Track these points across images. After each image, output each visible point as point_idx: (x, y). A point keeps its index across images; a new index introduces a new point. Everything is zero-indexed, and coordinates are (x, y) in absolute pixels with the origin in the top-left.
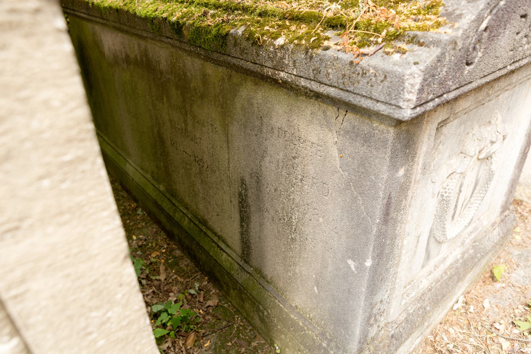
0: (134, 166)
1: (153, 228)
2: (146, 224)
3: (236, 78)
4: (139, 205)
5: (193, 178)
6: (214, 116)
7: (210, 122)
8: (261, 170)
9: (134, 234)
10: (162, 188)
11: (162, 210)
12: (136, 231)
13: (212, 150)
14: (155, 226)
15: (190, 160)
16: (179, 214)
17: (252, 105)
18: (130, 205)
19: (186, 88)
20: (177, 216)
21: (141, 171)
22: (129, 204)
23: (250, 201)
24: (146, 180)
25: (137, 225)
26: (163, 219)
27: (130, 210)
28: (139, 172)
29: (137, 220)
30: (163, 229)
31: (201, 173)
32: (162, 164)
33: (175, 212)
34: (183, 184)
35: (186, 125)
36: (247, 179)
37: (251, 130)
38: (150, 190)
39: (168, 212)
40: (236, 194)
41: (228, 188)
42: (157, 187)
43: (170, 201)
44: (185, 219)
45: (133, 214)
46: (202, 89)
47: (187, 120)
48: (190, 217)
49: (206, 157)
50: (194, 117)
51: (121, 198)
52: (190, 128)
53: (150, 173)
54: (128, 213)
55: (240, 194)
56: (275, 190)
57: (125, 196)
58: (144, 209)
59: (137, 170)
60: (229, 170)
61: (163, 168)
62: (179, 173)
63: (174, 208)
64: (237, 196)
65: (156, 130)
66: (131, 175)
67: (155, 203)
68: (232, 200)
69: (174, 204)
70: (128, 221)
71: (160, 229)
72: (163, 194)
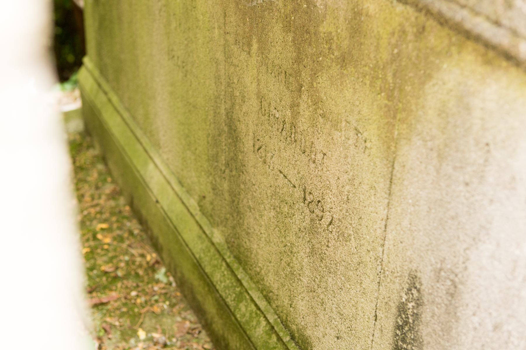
0: (165, 172)
1: (185, 319)
2: (172, 306)
3: (436, 37)
4: (162, 259)
5: (292, 238)
6: (365, 111)
7: (354, 124)
8: (466, 268)
9: (141, 326)
10: (218, 237)
11: (211, 286)
12: (147, 320)
13: (347, 188)
14: (191, 316)
15: (291, 196)
16: (246, 307)
17: (468, 108)
18: (143, 256)
19: (308, 32)
20: (243, 311)
21: (177, 187)
22: (140, 251)
23: (424, 331)
24: (185, 211)
25: (152, 305)
26: (210, 308)
27: (140, 266)
28: (173, 189)
29: (154, 293)
30: (207, 326)
31: (312, 230)
32: (226, 186)
33: (239, 298)
34: (268, 242)
35: (296, 115)
36: (426, 279)
37: (455, 168)
38: (190, 234)
39: (223, 294)
40: (392, 305)
41: (375, 286)
42: (208, 232)
43: (233, 272)
44: (259, 322)
45: (146, 278)
46: (346, 42)
47: (298, 106)
48: (271, 321)
49: (330, 200)
50: (317, 102)
51: (126, 235)
52: (303, 124)
53: (196, 197)
54: (137, 274)
55: (402, 309)
56: (496, 328)
57: (136, 232)
58: (172, 270)
59: (169, 183)
60: (383, 245)
61: (227, 196)
62: (261, 216)
63: (238, 289)
64: (394, 310)
65: (223, 107)
66: (155, 191)
67: (198, 266)
68: (380, 315)
69: (239, 281)
70: (134, 293)
71: (199, 325)
72: (218, 251)
